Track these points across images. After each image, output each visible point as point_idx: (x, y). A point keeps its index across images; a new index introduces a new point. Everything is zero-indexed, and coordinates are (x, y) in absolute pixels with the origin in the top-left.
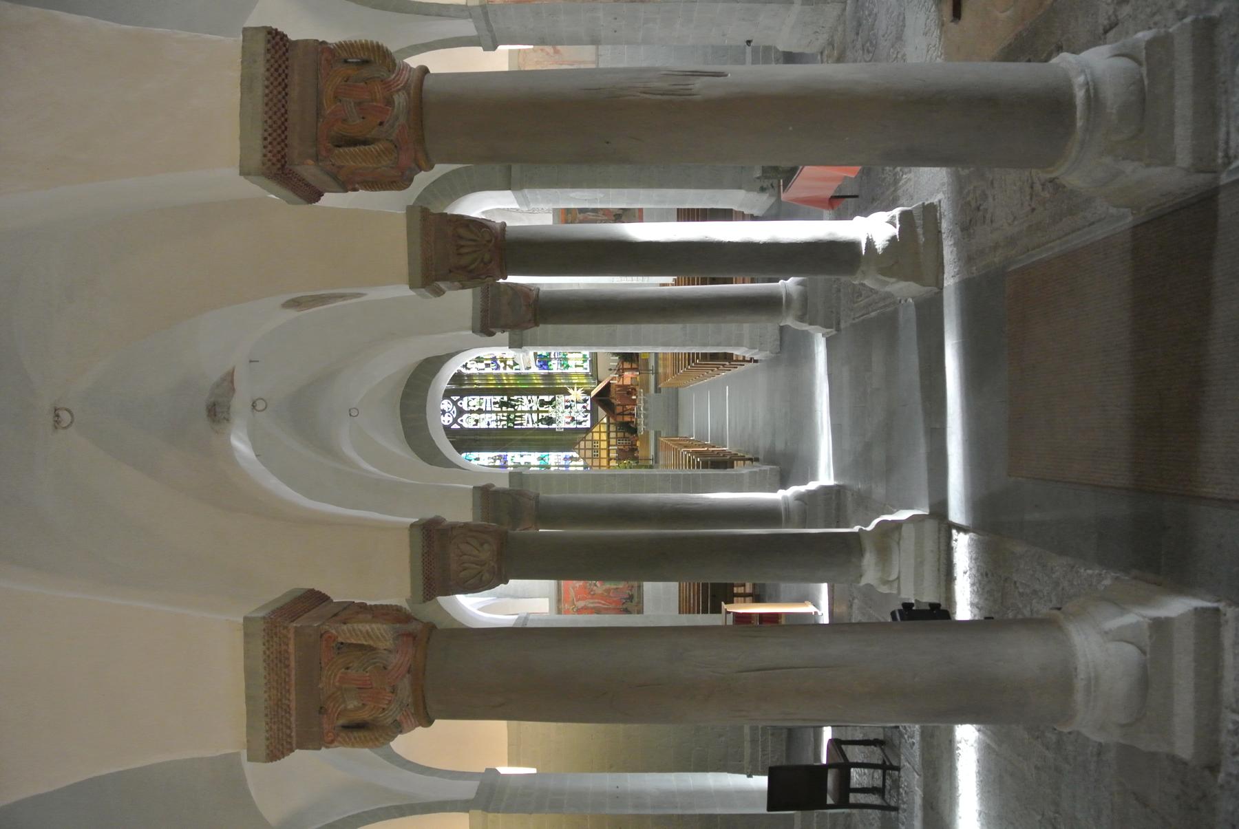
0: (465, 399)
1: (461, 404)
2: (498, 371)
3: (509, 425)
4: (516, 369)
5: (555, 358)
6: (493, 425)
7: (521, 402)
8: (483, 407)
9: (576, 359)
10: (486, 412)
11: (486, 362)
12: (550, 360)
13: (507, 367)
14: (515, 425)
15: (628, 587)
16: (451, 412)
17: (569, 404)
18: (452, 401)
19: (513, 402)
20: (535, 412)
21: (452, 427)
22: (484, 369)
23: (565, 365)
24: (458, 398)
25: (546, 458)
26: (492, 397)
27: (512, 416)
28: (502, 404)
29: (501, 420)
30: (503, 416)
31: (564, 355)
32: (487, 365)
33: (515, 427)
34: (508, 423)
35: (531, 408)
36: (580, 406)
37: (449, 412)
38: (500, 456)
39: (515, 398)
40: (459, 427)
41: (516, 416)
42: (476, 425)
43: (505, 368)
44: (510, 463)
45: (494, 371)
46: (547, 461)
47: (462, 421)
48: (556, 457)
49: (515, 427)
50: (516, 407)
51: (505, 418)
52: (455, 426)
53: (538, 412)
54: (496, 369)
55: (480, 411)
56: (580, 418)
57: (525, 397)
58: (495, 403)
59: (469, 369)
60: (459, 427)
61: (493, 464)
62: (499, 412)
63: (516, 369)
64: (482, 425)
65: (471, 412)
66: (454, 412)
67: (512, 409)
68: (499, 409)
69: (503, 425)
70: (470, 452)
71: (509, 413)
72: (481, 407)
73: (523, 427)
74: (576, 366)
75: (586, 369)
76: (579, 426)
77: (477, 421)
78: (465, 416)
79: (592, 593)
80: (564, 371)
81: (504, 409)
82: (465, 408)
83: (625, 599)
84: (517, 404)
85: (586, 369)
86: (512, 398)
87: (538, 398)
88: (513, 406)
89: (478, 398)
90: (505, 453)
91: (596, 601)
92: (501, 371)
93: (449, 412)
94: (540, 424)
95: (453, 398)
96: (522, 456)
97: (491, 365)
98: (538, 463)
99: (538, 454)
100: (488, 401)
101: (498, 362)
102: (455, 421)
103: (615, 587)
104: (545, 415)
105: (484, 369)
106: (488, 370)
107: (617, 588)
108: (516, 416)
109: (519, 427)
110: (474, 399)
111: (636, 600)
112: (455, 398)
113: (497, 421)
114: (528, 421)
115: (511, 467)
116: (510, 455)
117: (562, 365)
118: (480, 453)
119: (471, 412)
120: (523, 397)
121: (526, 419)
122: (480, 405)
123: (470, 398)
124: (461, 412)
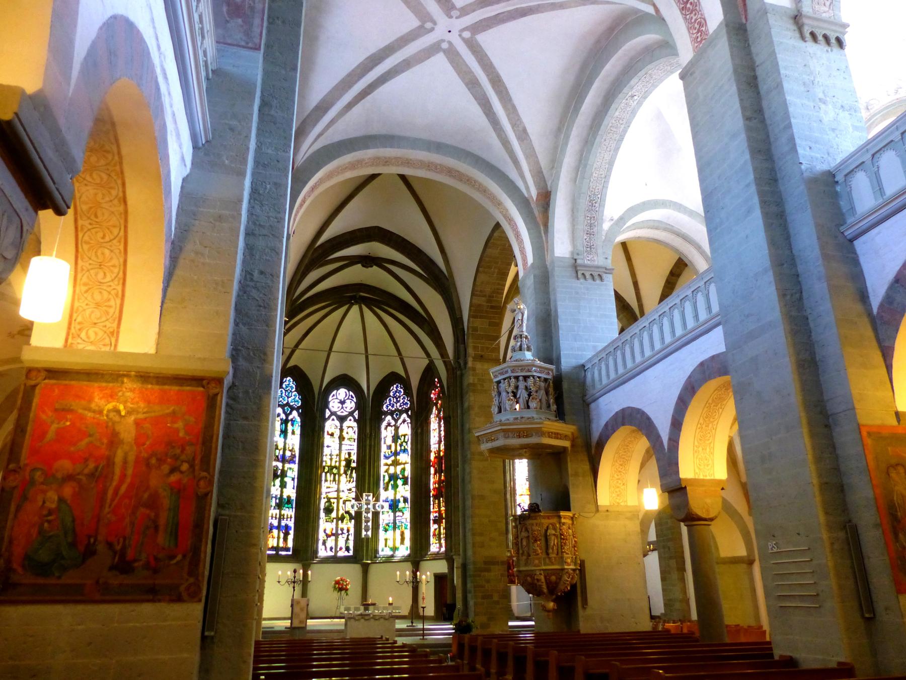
0: (355, 425)
1: (350, 420)
2: (382, 457)
3: (327, 468)
4: (384, 476)
5: (395, 517)
6: (326, 451)
7: (350, 481)
8: (346, 442)
9: (394, 540)
10: (340, 445)
11: (393, 445)
12: (394, 512)
13: (387, 467)
14: (326, 473)
15: (156, 559)
16: (342, 410)
17: (345, 531)
18: (354, 412)
19: (349, 473)
20: (338, 495)
21: (327, 410)
22: (385, 443)
23: (387, 527)
24: (357, 417)
25: (290, 506)
26: (355, 451)
27: (335, 471)
28: (348, 462)
29: (331, 459)
30: (336, 462)
31: (399, 527)
32: (389, 447)
33: (324, 474)
34: (328, 466)
35: (343, 491)
36: (341, 542)
37: (342, 408)
38: (294, 456)
39: (354, 475)
40: (327, 417)
41: (335, 475)
42: (328, 434)
43: (386, 465)
44: (287, 466)
45: (382, 454)
46: (286, 506)
47: (333, 420)
48: (289, 516)
49: (324, 474)
50: (344, 475)
51: (333, 464)
52: (328, 413)
53: (338, 498)
54: (385, 456)
55: (341, 438)
56: (331, 542)
57: (354, 484)
58: (349, 454)
59: (386, 429)
60: (327, 417)
61: (287, 448)
62: (340, 458)
63: (384, 476)
64: (327, 440)
65: (341, 430)
66: (342, 412)
67: (342, 471)
68: (343, 458)
69: (326, 461)
70: (301, 426)
71: (338, 468)
72: (346, 439)
73: (323, 482)
74: (386, 540)
75: (382, 550)
76: (320, 542)
77: (332, 435)
78: (337, 423)
79: (153, 461)
80: (381, 526)
81: (343, 463)
82: (346, 424)
83: (124, 548)
84: (348, 476)
85: (382, 550)
86: (354, 471)
87: (353, 499)
88: (345, 473)
89: (356, 437)
90: (297, 462)
91: (130, 472)
92: (383, 461)
93: (342, 408)
94: (326, 500)
95: (357, 412)
96: (293, 479)
97: (389, 451)
98: (285, 496)
99: (293, 496)
100: (351, 447)
101: (393, 458)
102: (333, 413)
103: (162, 521)
104: (335, 506)
105: (385, 443)
106: (384, 448)
107: (156, 528)
108: (335, 475)
109: (323, 478)
110: (354, 432)
111: (116, 580)
112: (356, 414)
113: (331, 455)
114: (329, 488)
115: (283, 467)
116: (295, 467)
117: (387, 525)
118: (299, 436)
119: (341, 430)
120: (355, 483)
121: (331, 486)
122: (349, 439)
123: (356, 429)
124: (342, 419)
